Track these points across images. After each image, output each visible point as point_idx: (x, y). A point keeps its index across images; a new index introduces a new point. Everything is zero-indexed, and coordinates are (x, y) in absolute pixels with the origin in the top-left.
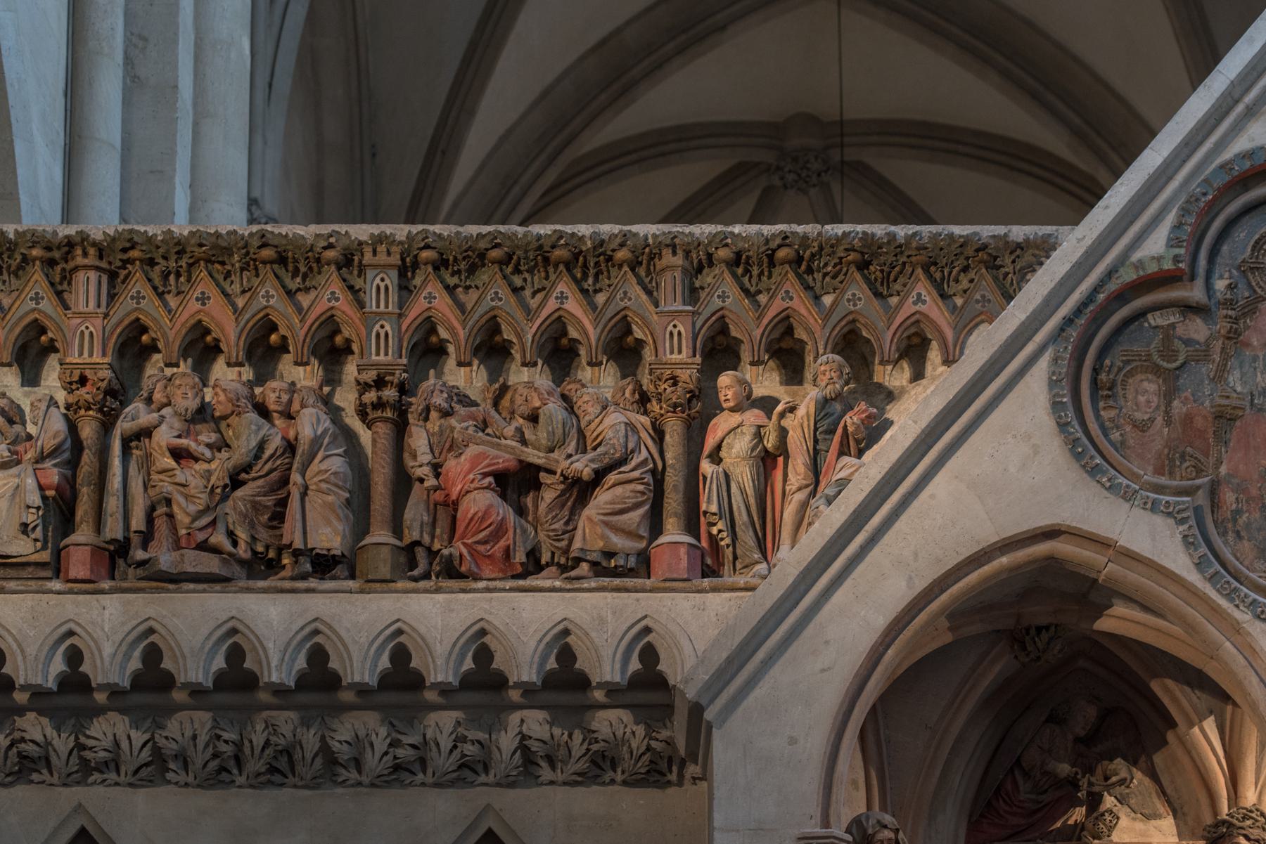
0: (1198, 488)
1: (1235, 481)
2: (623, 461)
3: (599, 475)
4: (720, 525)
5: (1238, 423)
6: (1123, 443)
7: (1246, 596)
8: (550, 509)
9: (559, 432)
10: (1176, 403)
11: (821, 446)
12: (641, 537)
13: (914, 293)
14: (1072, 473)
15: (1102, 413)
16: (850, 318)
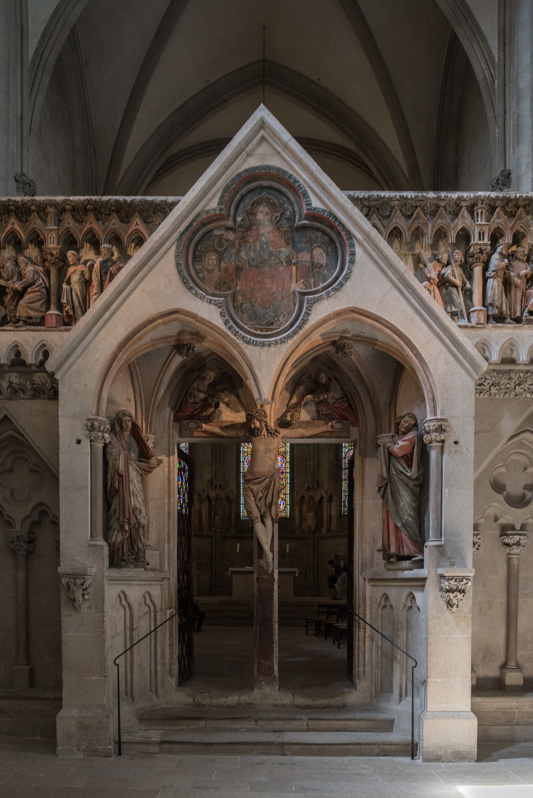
0: (228, 294)
1: (242, 292)
2: (33, 284)
3: (25, 289)
4: (68, 307)
5: (244, 271)
6: (204, 278)
7: (241, 334)
8: (9, 301)
9: (11, 273)
10: (222, 263)
11: (103, 278)
12: (42, 312)
13: (135, 222)
14: (183, 289)
15: (197, 267)
16: (113, 231)
